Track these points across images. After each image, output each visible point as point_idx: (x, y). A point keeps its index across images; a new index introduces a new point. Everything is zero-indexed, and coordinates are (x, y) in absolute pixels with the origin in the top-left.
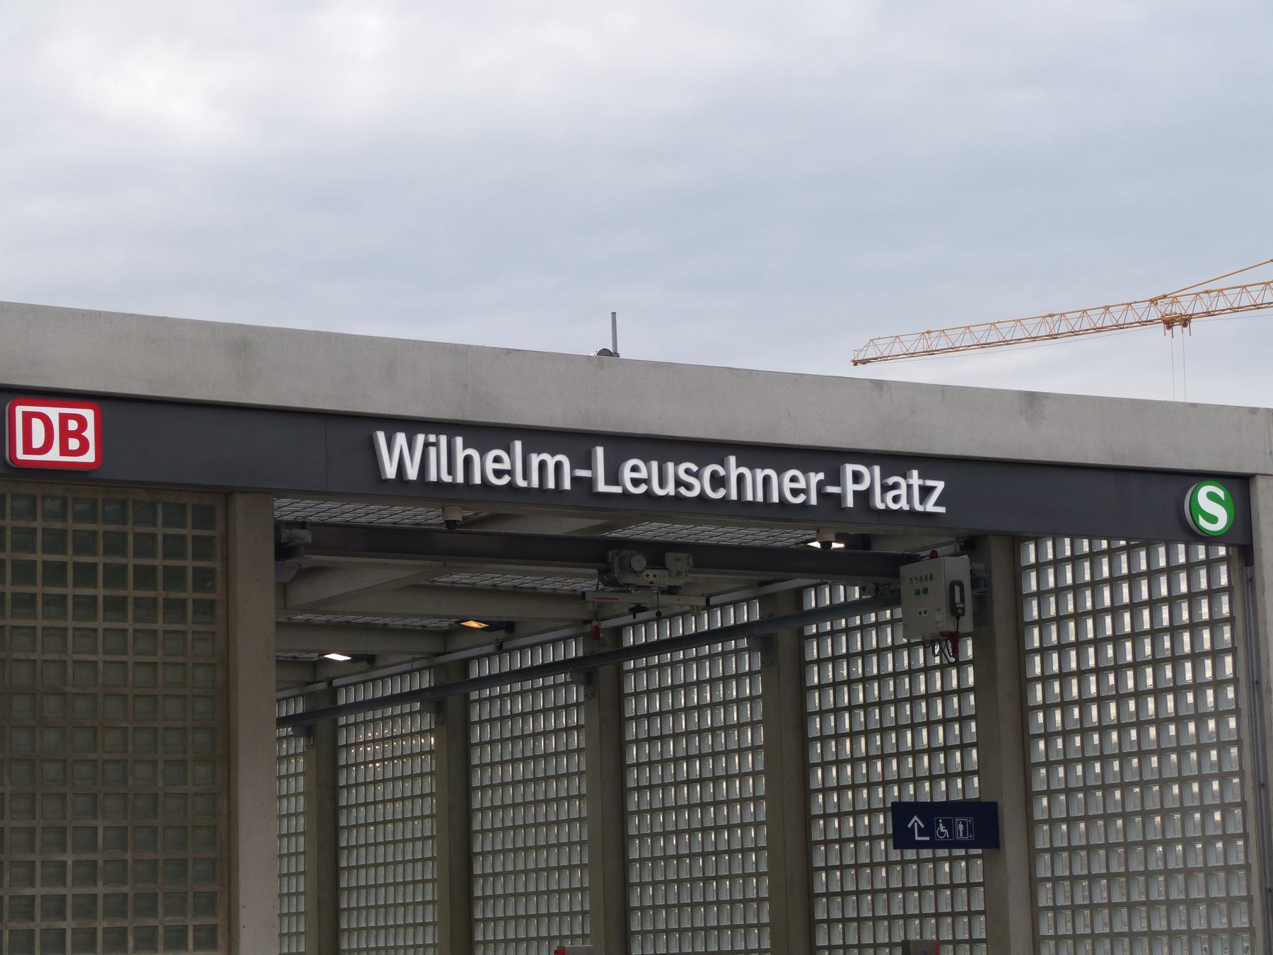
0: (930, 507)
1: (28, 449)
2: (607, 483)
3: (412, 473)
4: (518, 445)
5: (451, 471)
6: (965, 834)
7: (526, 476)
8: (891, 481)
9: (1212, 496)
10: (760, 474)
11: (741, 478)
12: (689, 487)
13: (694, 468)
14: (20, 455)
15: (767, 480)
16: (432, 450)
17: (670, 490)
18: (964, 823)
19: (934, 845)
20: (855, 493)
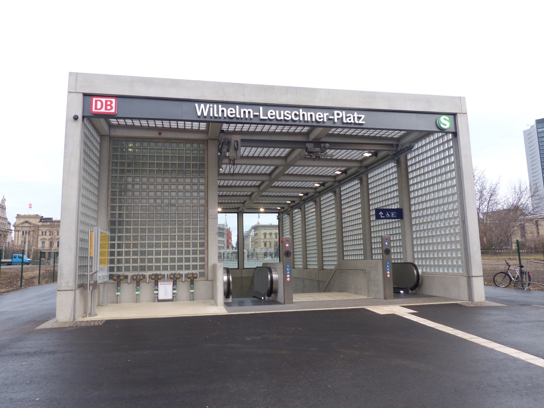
0: (360, 122)
1: (96, 108)
2: (263, 116)
3: (205, 114)
4: (237, 107)
5: (218, 113)
6: (394, 216)
7: (240, 114)
8: (348, 115)
9: (445, 119)
10: (309, 114)
11: (303, 115)
12: (288, 117)
13: (289, 112)
14: (94, 110)
15: (311, 116)
16: (211, 109)
17: (282, 118)
18: (394, 213)
19: (386, 218)
20: (338, 119)
